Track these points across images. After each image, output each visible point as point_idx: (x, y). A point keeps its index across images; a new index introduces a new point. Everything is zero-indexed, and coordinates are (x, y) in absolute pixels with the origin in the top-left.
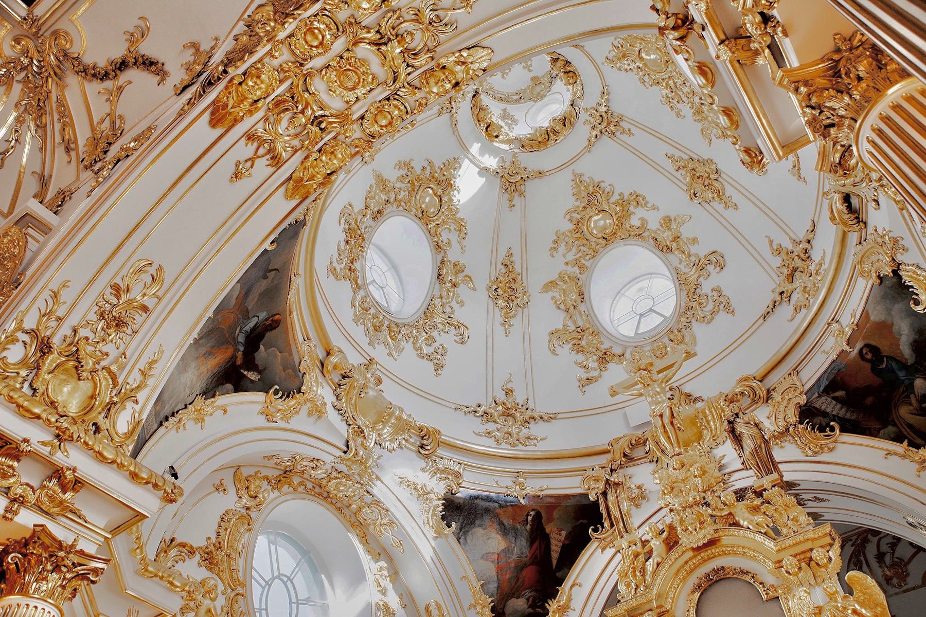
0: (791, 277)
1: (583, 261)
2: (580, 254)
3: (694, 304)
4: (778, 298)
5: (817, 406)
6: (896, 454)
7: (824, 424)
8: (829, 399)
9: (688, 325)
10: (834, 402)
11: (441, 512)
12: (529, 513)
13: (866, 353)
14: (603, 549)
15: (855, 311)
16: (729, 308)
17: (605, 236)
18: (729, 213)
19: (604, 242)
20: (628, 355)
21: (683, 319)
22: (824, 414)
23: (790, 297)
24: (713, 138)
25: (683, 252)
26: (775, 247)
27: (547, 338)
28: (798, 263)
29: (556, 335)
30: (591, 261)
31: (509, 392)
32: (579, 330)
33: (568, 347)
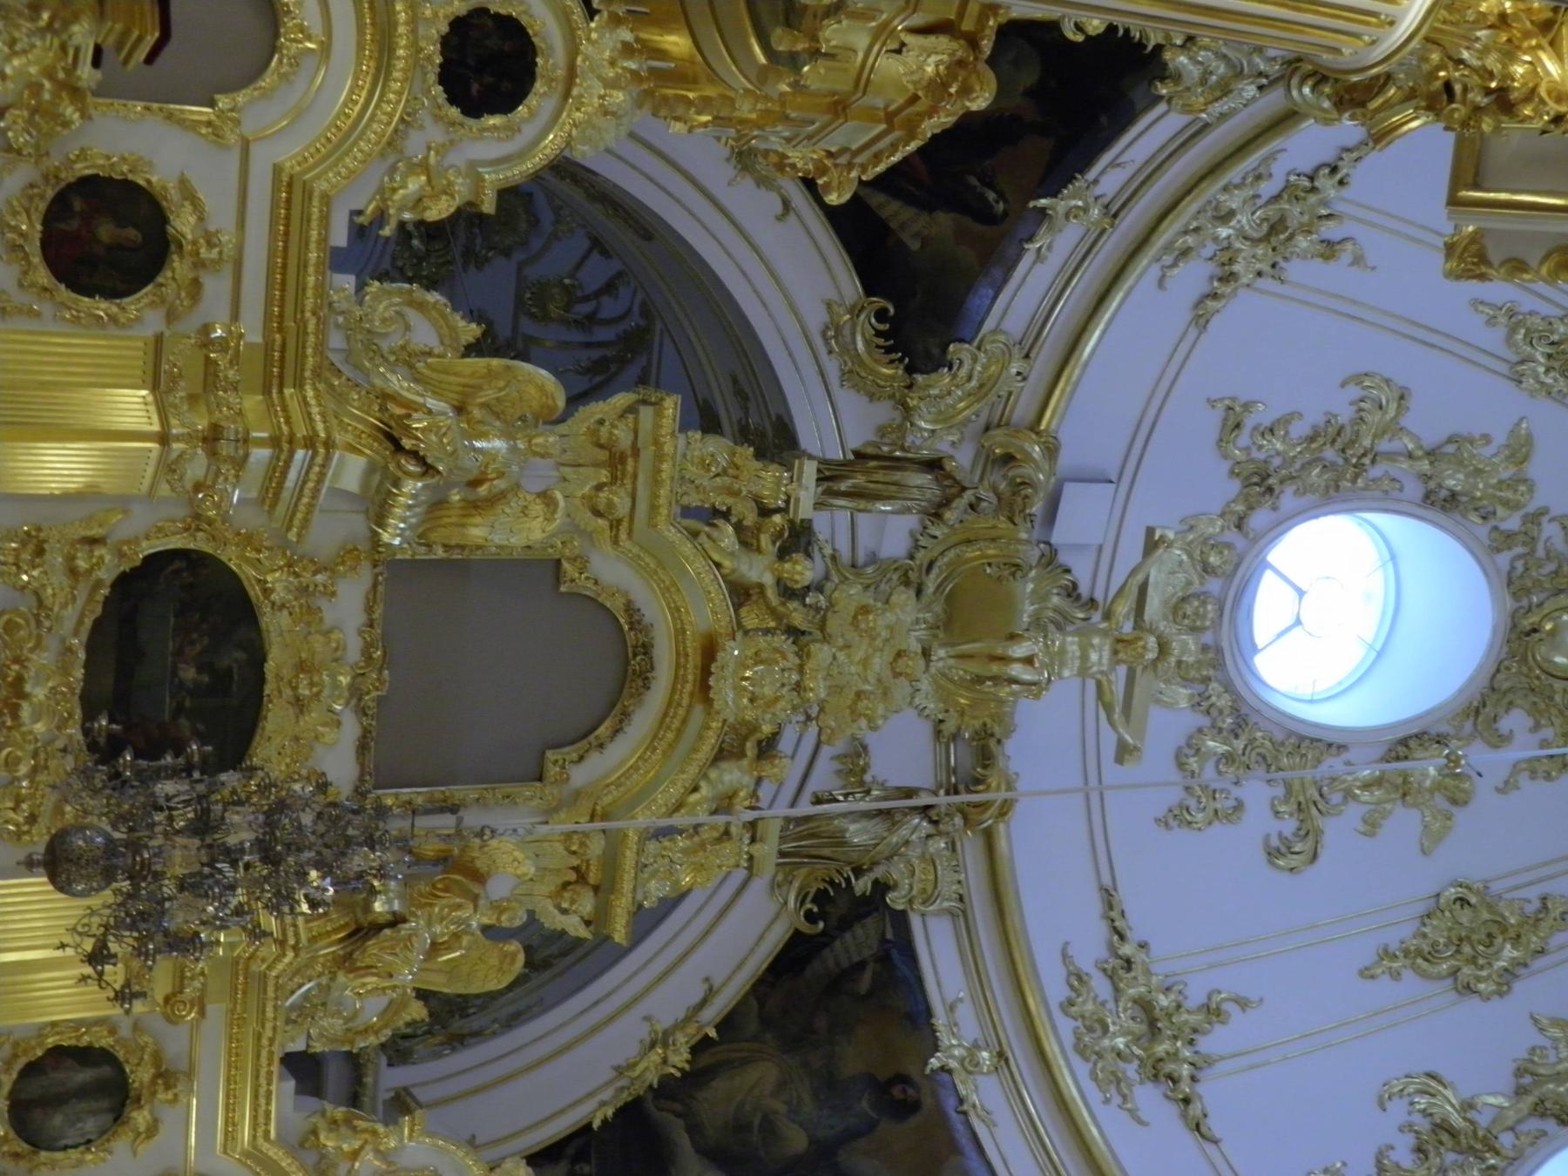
0: (1144, 1005)
1: (1519, 550)
2: (1540, 553)
3: (1239, 744)
4: (1126, 950)
5: (869, 921)
6: (704, 1003)
7: (829, 908)
8: (867, 953)
9: (1205, 704)
10: (856, 959)
11: (1127, 31)
12: (1006, 201)
13: (904, 1091)
14: (829, 306)
15: (991, 1125)
16: (1178, 817)
17: (1537, 636)
18: (1366, 953)
19: (1526, 623)
20: (1232, 536)
21: (1224, 701)
22: (845, 924)
23: (1111, 978)
24: (1540, 1040)
25: (1366, 786)
26: (1226, 1006)
27: (1400, 380)
28: (1161, 1049)
29: (1393, 406)
30: (1505, 568)
31: (1329, 249)
32: (1367, 461)
33: (1345, 415)
